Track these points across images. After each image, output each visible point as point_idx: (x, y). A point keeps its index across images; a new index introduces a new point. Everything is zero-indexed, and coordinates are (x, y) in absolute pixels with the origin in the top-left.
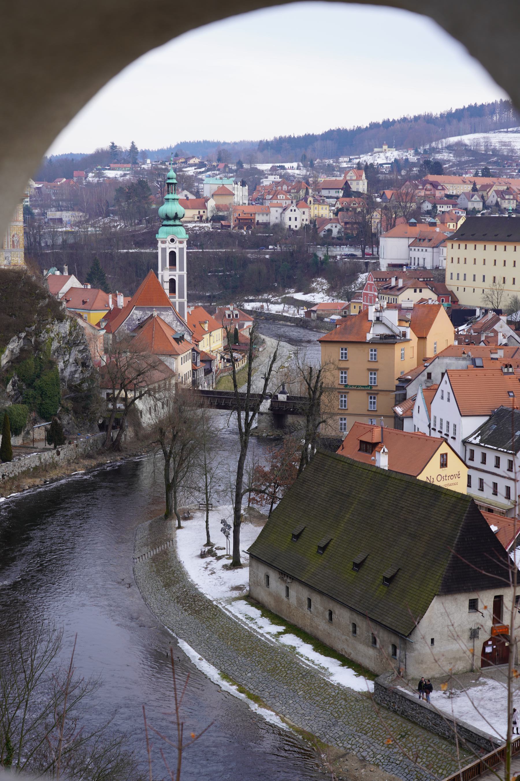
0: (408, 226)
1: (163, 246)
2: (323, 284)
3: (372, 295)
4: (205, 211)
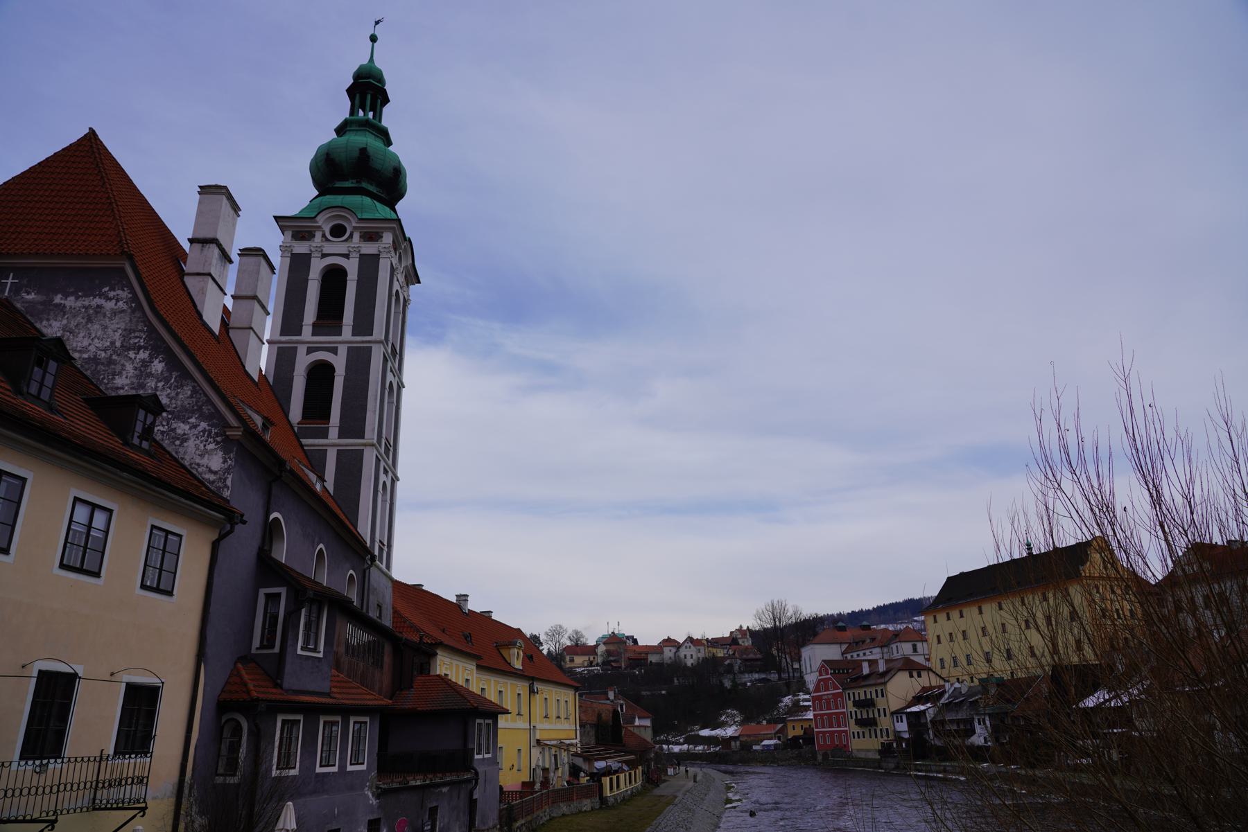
0: (836, 631)
1: (301, 248)
2: (733, 716)
3: (830, 697)
4: (596, 657)
